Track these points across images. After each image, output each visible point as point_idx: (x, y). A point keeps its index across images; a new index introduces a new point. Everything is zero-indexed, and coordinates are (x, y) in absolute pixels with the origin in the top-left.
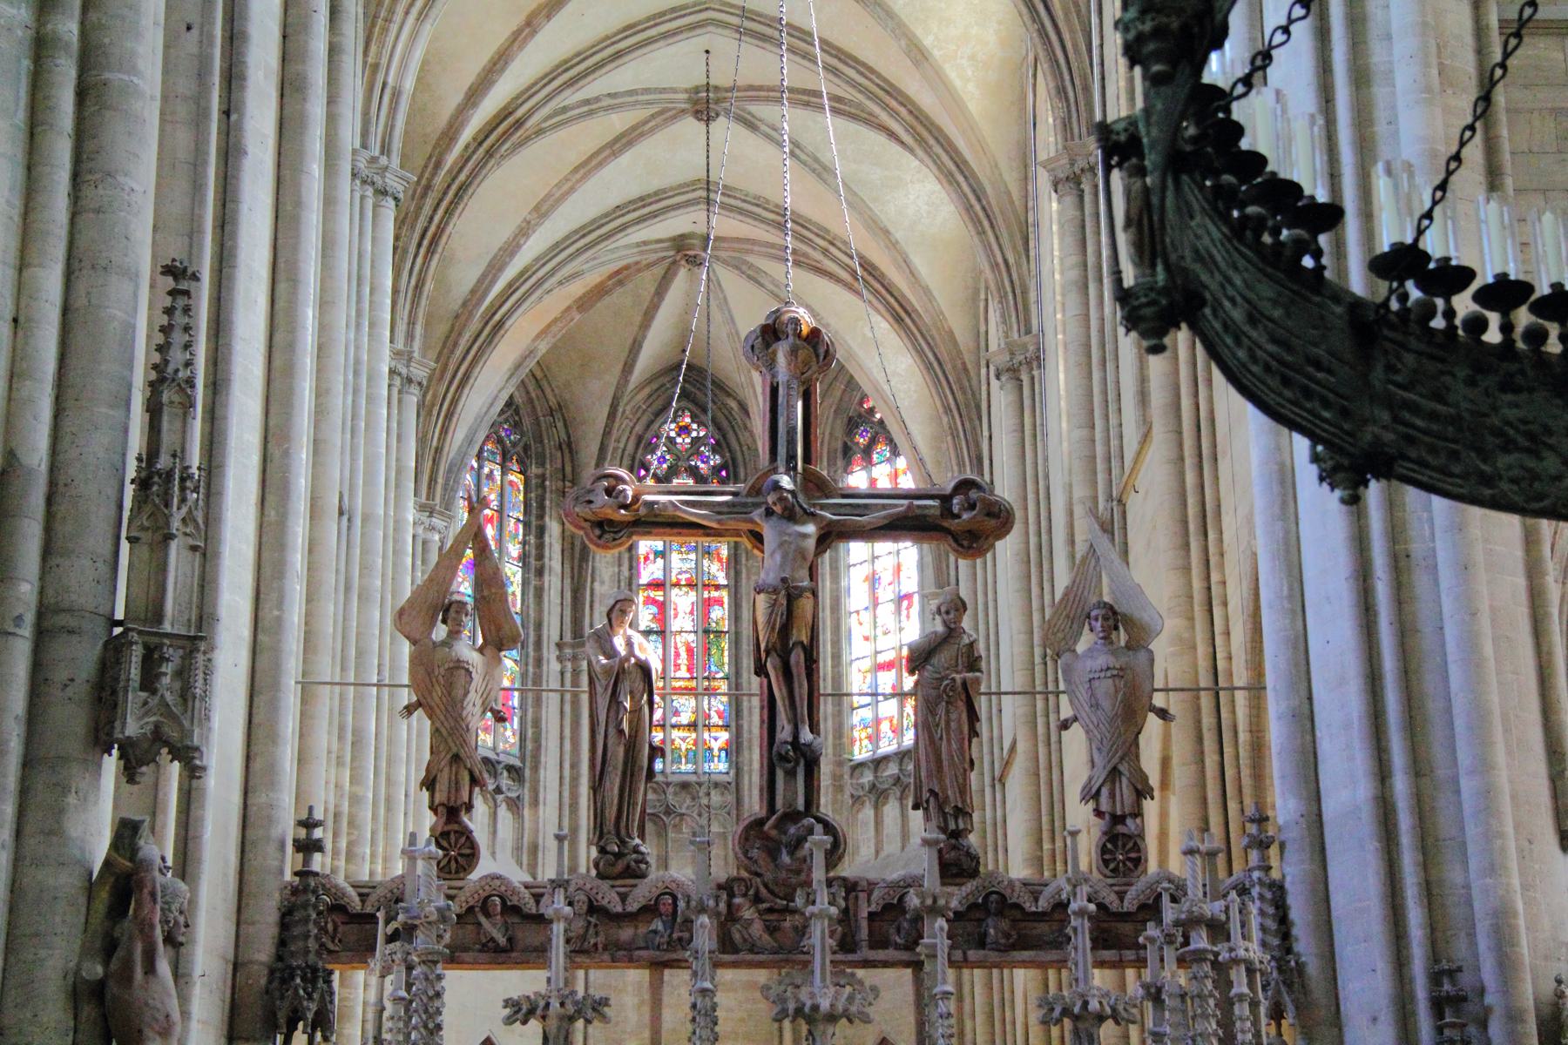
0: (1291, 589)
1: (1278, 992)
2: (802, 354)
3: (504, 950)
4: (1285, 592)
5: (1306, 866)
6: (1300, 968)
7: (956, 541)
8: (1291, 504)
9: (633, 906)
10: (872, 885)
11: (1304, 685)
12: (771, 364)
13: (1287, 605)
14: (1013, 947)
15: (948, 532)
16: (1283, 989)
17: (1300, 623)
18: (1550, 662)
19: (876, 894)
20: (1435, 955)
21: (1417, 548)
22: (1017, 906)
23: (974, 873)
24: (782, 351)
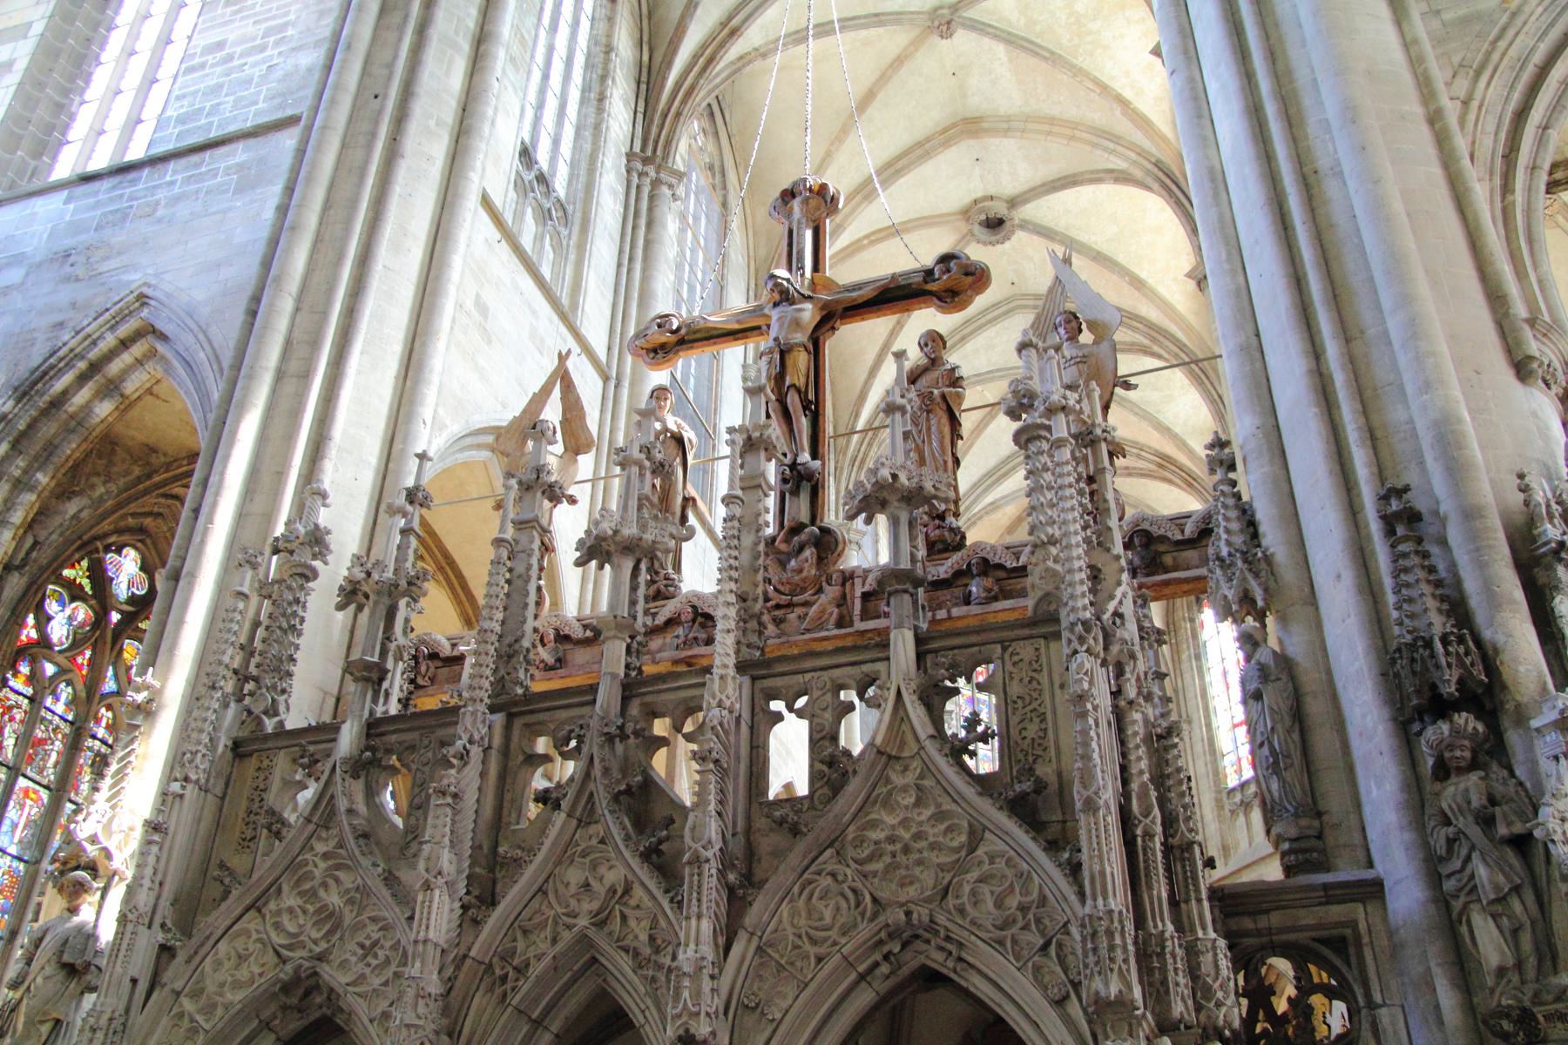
0: (1229, 254)
1: (1245, 579)
2: (813, 203)
3: (552, 668)
4: (1224, 255)
5: (1266, 469)
6: (1268, 559)
7: (940, 299)
8: (1224, 195)
9: (660, 620)
10: (867, 572)
11: (1252, 325)
12: (789, 215)
13: (1226, 266)
14: (995, 599)
15: (931, 293)
16: (1249, 576)
17: (1241, 279)
18: (1478, 228)
19: (869, 580)
20: (1381, 474)
21: (1323, 163)
22: (1000, 567)
23: (960, 545)
24: (796, 205)
